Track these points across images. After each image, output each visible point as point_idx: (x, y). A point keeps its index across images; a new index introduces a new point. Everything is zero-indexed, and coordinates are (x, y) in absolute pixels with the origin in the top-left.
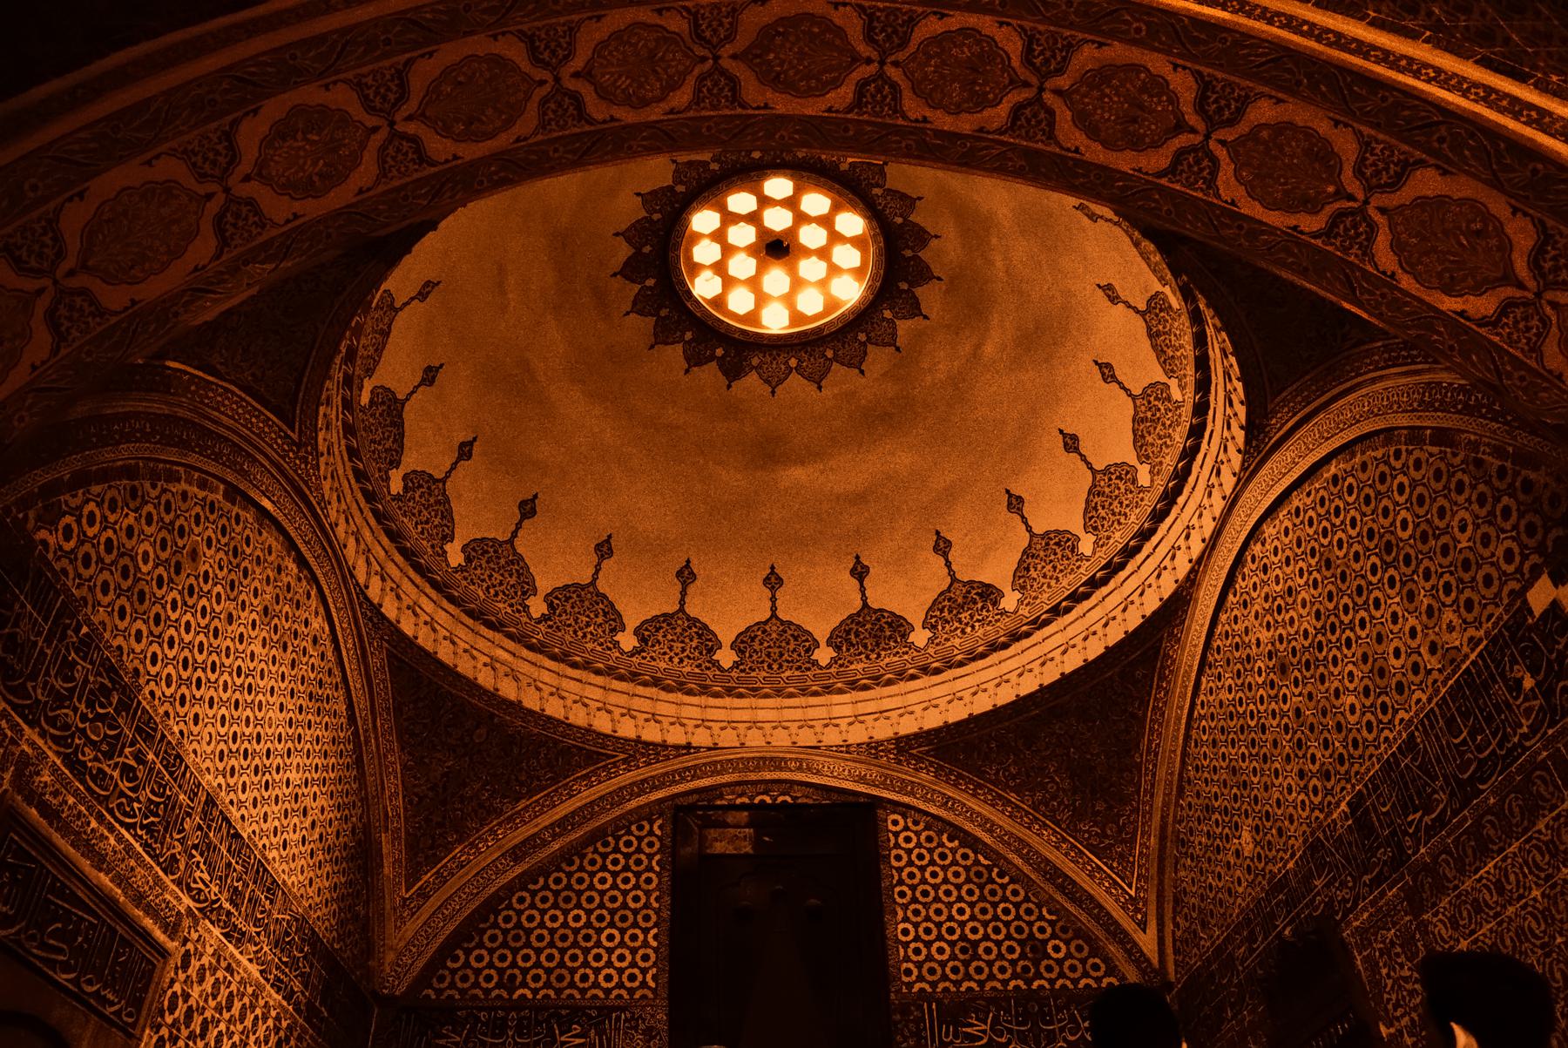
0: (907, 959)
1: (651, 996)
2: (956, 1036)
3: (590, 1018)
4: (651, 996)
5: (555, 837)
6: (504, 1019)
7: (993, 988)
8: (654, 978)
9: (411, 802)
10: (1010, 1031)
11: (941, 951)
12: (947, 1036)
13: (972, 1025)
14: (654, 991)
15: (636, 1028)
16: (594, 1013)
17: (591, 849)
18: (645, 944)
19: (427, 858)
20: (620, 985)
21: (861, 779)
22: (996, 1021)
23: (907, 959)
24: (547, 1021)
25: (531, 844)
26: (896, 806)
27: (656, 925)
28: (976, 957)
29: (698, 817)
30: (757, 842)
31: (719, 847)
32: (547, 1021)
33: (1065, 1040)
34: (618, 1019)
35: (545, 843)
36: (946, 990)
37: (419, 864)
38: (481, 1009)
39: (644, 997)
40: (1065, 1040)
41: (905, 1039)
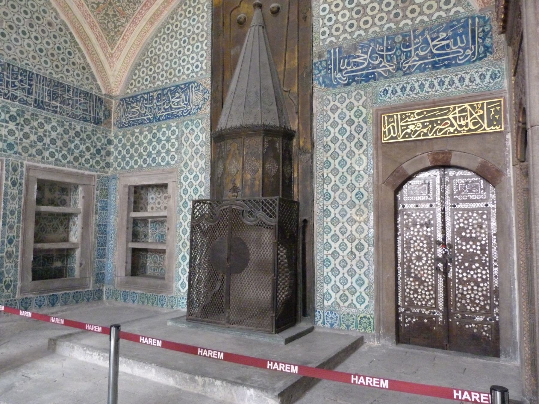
0: (324, 25)
1: (204, 73)
2: (348, 64)
3: (182, 89)
4: (204, 73)
5: (165, 8)
6: (152, 96)
7: (375, 32)
8: (206, 65)
9: (93, 7)
10: (382, 56)
11: (345, 16)
12: (343, 66)
13: (358, 57)
14: (206, 71)
15: (198, 90)
16: (183, 86)
17: (180, 9)
18: (202, 49)
19: (115, 33)
20: (193, 71)
22: (374, 51)
23: (324, 25)
24: (167, 94)
25: (156, 15)
27: (206, 39)
28: (365, 14)
32: (167, 94)
33: (417, 55)
34: (192, 87)
35: (162, 12)
36: (345, 38)
37: (113, 36)
38: (145, 94)
39: (202, 74)
40: (417, 55)
41: (320, 71)
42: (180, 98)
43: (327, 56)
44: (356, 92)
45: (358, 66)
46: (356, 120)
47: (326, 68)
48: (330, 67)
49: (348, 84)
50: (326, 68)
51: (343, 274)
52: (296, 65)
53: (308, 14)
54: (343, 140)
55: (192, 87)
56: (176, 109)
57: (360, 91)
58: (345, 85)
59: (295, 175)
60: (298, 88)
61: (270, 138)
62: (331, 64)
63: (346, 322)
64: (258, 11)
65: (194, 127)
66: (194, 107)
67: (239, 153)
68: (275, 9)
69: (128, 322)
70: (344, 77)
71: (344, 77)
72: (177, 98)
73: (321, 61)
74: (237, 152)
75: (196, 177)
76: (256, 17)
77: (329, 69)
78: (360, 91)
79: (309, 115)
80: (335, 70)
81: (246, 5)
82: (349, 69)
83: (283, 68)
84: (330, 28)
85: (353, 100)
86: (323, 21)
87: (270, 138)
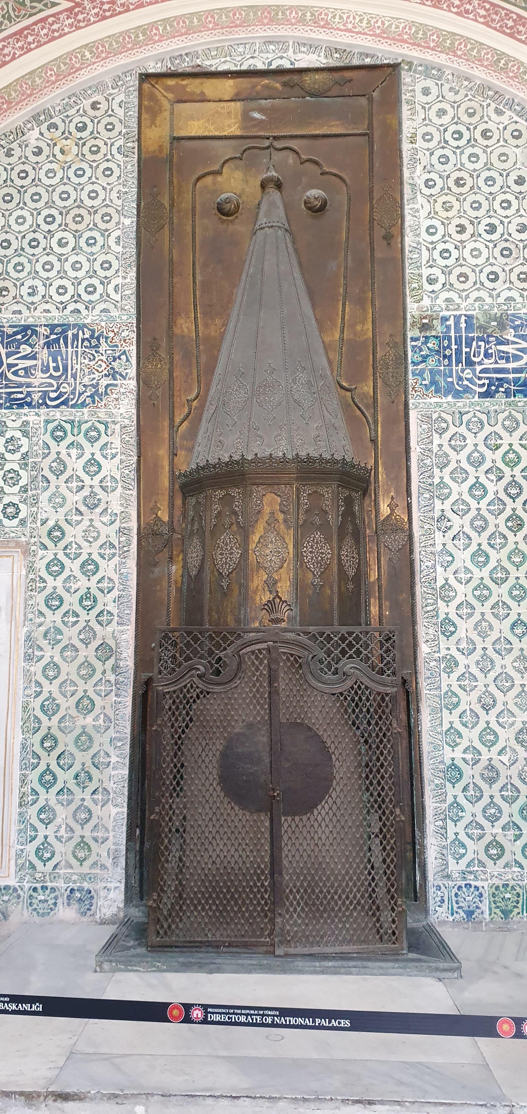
13: (507, 342)
21: (384, 34)
26: (429, 70)
29: (168, 89)
30: (246, 116)
31: (195, 128)
34: (76, 337)
42: (34, 358)
43: (439, 329)
44: (506, 413)
45: (508, 361)
46: (507, 470)
47: (438, 352)
48: (447, 352)
49: (487, 394)
50: (438, 352)
51: (492, 797)
52: (370, 334)
53: (395, 231)
54: (479, 509)
55: (76, 337)
56: (20, 385)
57: (514, 413)
58: (482, 395)
59: (373, 576)
60: (375, 387)
61: (347, 493)
62: (449, 347)
63: (502, 904)
64: (275, 195)
65: (81, 439)
66: (80, 388)
67: (285, 521)
68: (318, 204)
69: (209, 944)
70: (480, 378)
71: (480, 378)
72: (25, 357)
73: (426, 337)
74: (281, 517)
75: (90, 568)
76: (274, 209)
77: (445, 356)
78: (514, 413)
79: (402, 448)
80: (458, 361)
81: (238, 175)
82: (488, 363)
83: (337, 336)
84: (447, 271)
85: (498, 429)
86: (431, 255)
87: (347, 493)
